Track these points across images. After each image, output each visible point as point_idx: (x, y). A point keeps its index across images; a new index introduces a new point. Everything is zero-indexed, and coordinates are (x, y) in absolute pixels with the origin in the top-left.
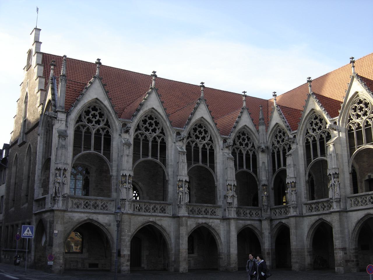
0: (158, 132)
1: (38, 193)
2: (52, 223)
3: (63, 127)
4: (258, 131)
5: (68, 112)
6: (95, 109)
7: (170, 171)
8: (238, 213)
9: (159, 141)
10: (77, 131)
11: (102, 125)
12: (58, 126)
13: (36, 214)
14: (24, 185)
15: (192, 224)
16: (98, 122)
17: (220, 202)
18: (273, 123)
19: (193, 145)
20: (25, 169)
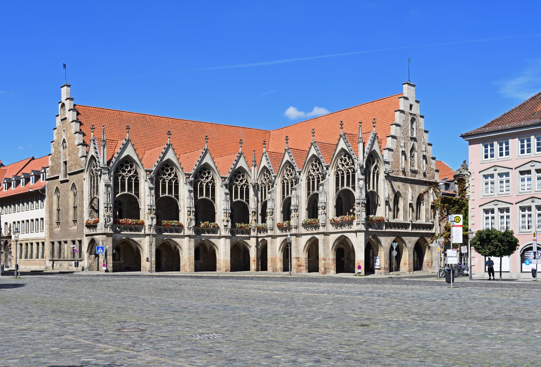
0: (173, 175)
9: (174, 182)
13: (87, 235)
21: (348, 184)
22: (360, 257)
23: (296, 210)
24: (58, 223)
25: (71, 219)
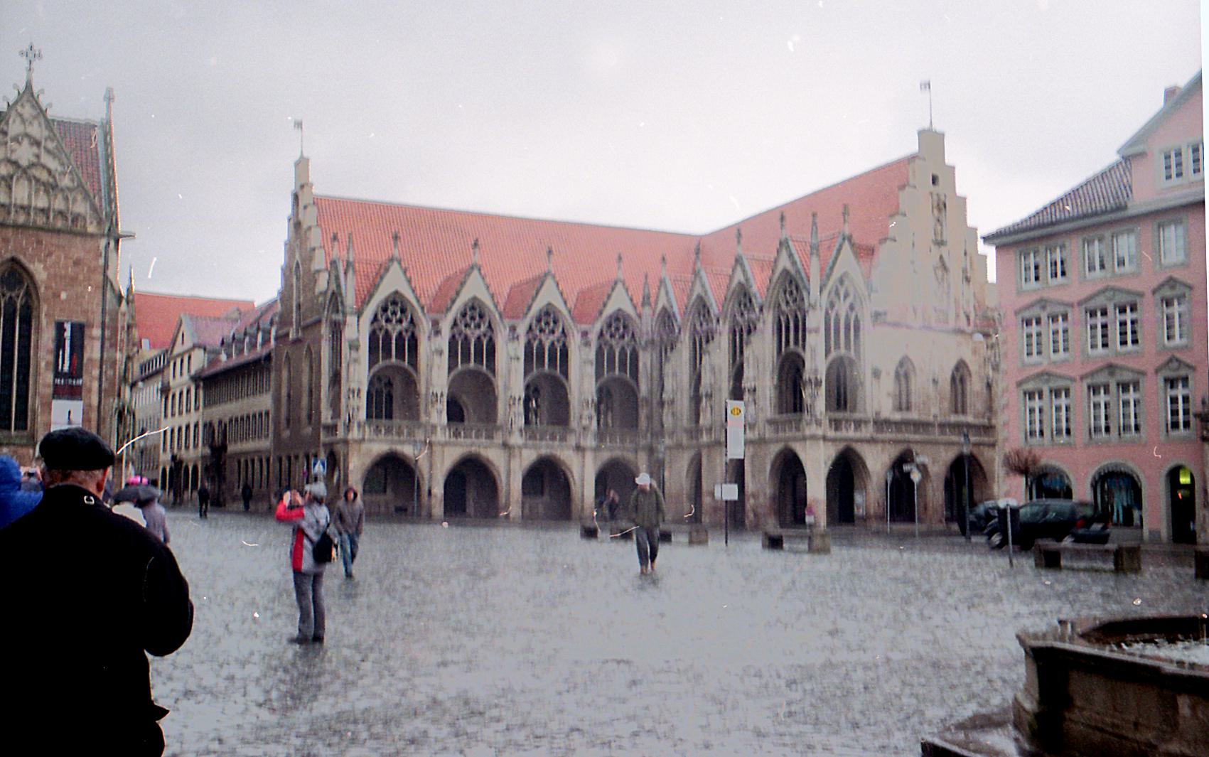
0: (483, 328)
1: (326, 416)
2: (346, 456)
3: (354, 336)
4: (640, 316)
5: (359, 314)
6: (394, 303)
7: (499, 382)
8: (600, 436)
10: (373, 337)
11: (405, 324)
12: (349, 333)
14: (305, 401)
15: (529, 457)
16: (400, 321)
17: (574, 423)
18: (660, 306)
19: (535, 344)
20: (305, 379)
21: (796, 342)
22: (816, 489)
23: (709, 396)
24: (288, 420)
25: (304, 414)
